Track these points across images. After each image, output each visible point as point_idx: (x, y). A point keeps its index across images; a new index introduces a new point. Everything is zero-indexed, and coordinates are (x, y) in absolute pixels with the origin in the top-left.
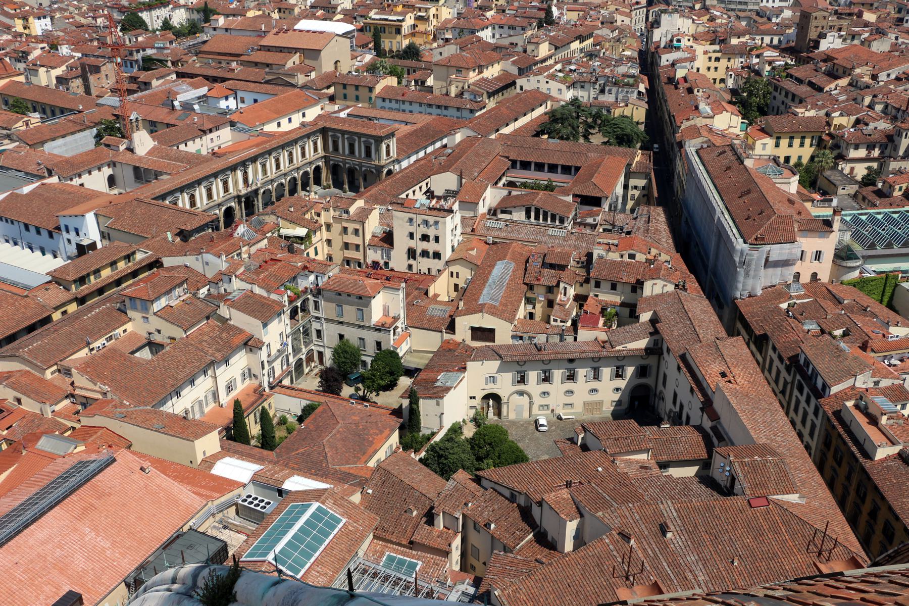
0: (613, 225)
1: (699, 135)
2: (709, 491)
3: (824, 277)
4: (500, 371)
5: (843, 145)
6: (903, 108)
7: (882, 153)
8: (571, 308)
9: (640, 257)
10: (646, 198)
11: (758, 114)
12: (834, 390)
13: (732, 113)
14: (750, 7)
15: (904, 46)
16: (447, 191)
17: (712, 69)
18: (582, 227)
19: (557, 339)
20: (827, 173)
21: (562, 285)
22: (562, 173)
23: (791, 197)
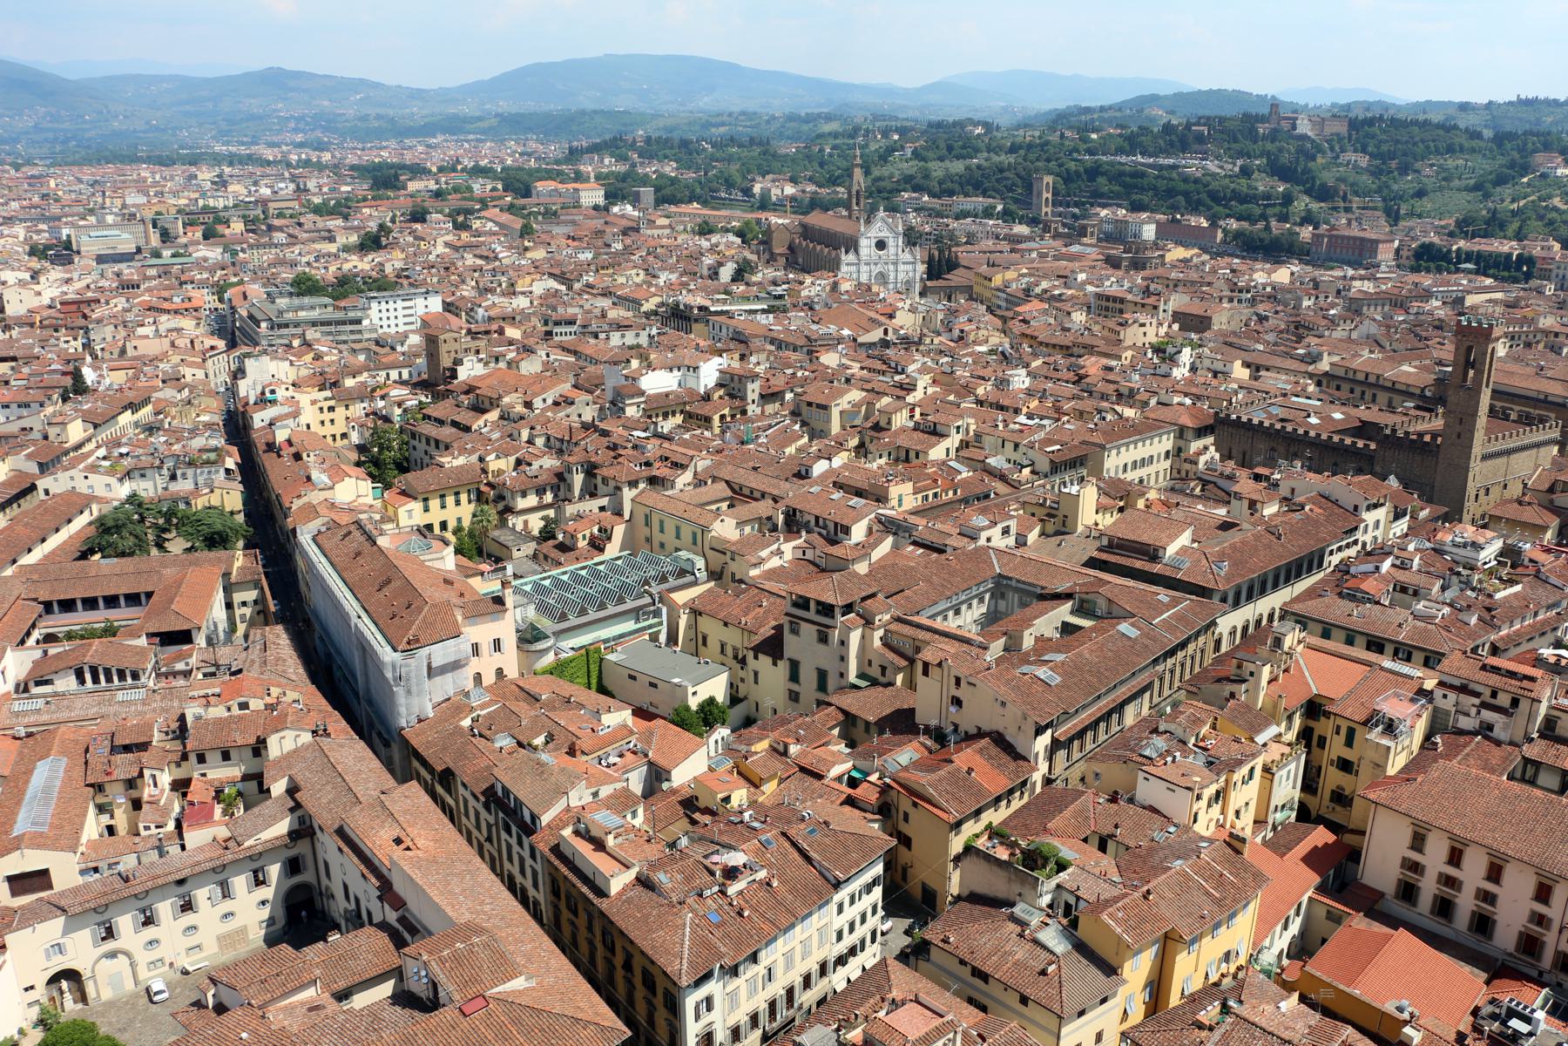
0: (217, 666)
1: (317, 515)
2: (408, 1011)
3: (512, 672)
5: (508, 495)
6: (567, 438)
7: (556, 496)
8: (170, 802)
9: (256, 704)
10: (262, 616)
12: (545, 819)
14: (367, 336)
15: (557, 364)
17: (327, 423)
18: (171, 678)
19: (154, 855)
20: (496, 534)
21: (147, 773)
22: (127, 606)
23: (449, 577)
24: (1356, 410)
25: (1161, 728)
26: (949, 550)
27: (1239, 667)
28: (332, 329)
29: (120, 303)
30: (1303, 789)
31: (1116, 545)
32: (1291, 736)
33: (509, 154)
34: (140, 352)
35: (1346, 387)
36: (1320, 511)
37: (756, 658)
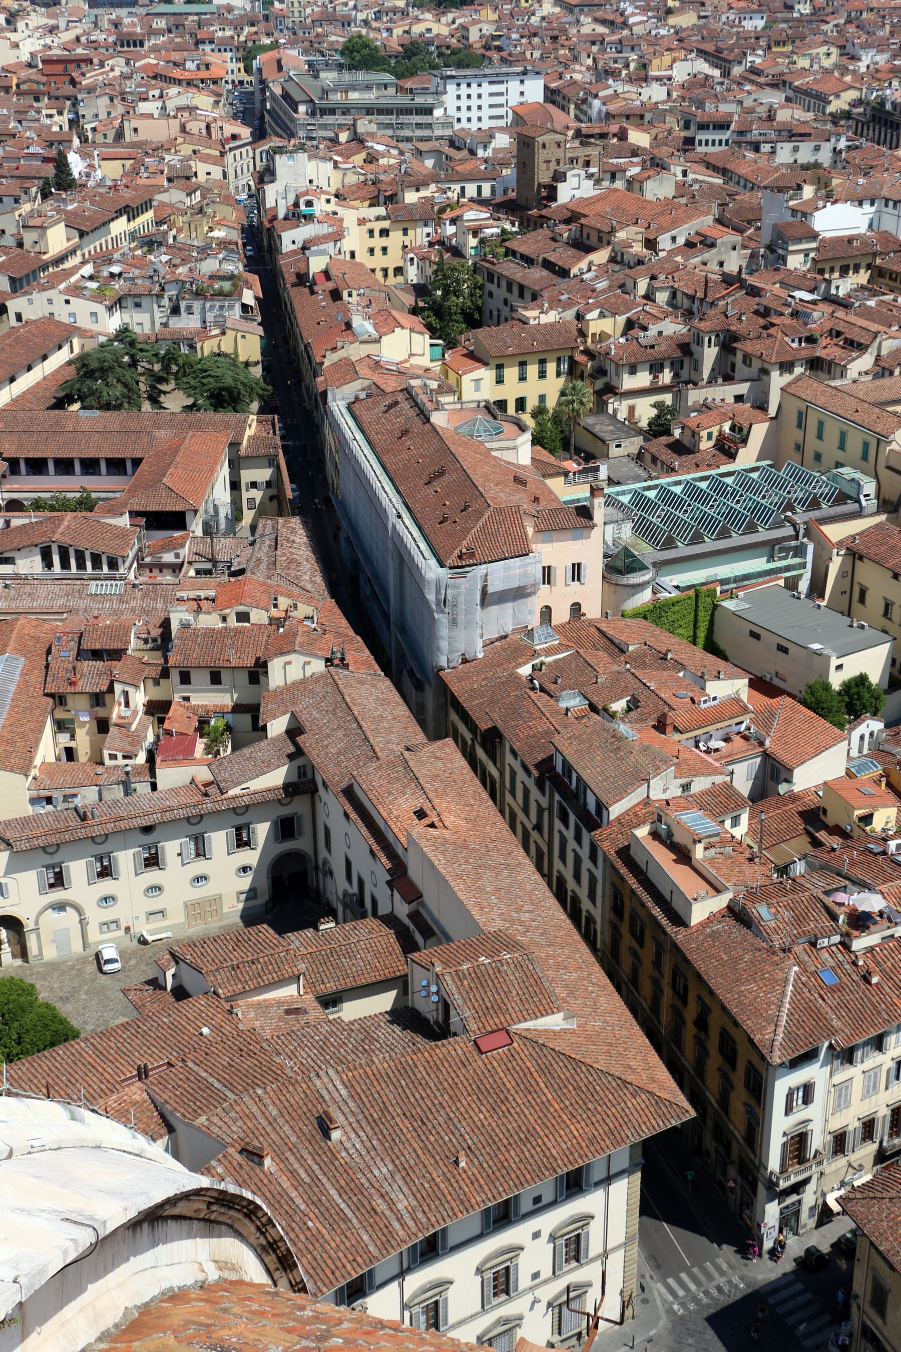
0: (214, 561)
1: (356, 376)
2: (408, 1035)
3: (592, 610)
4: (11, 869)
5: (611, 369)
6: (700, 295)
7: (676, 375)
8: (143, 727)
9: (258, 616)
10: (275, 502)
11: (464, 326)
12: (615, 811)
14: (438, 132)
15: (696, 187)
17: (378, 252)
18: (156, 571)
19: (119, 791)
20: (590, 421)
21: (118, 688)
22: (109, 474)
23: (521, 473)
28: (392, 119)
34: (142, 136)
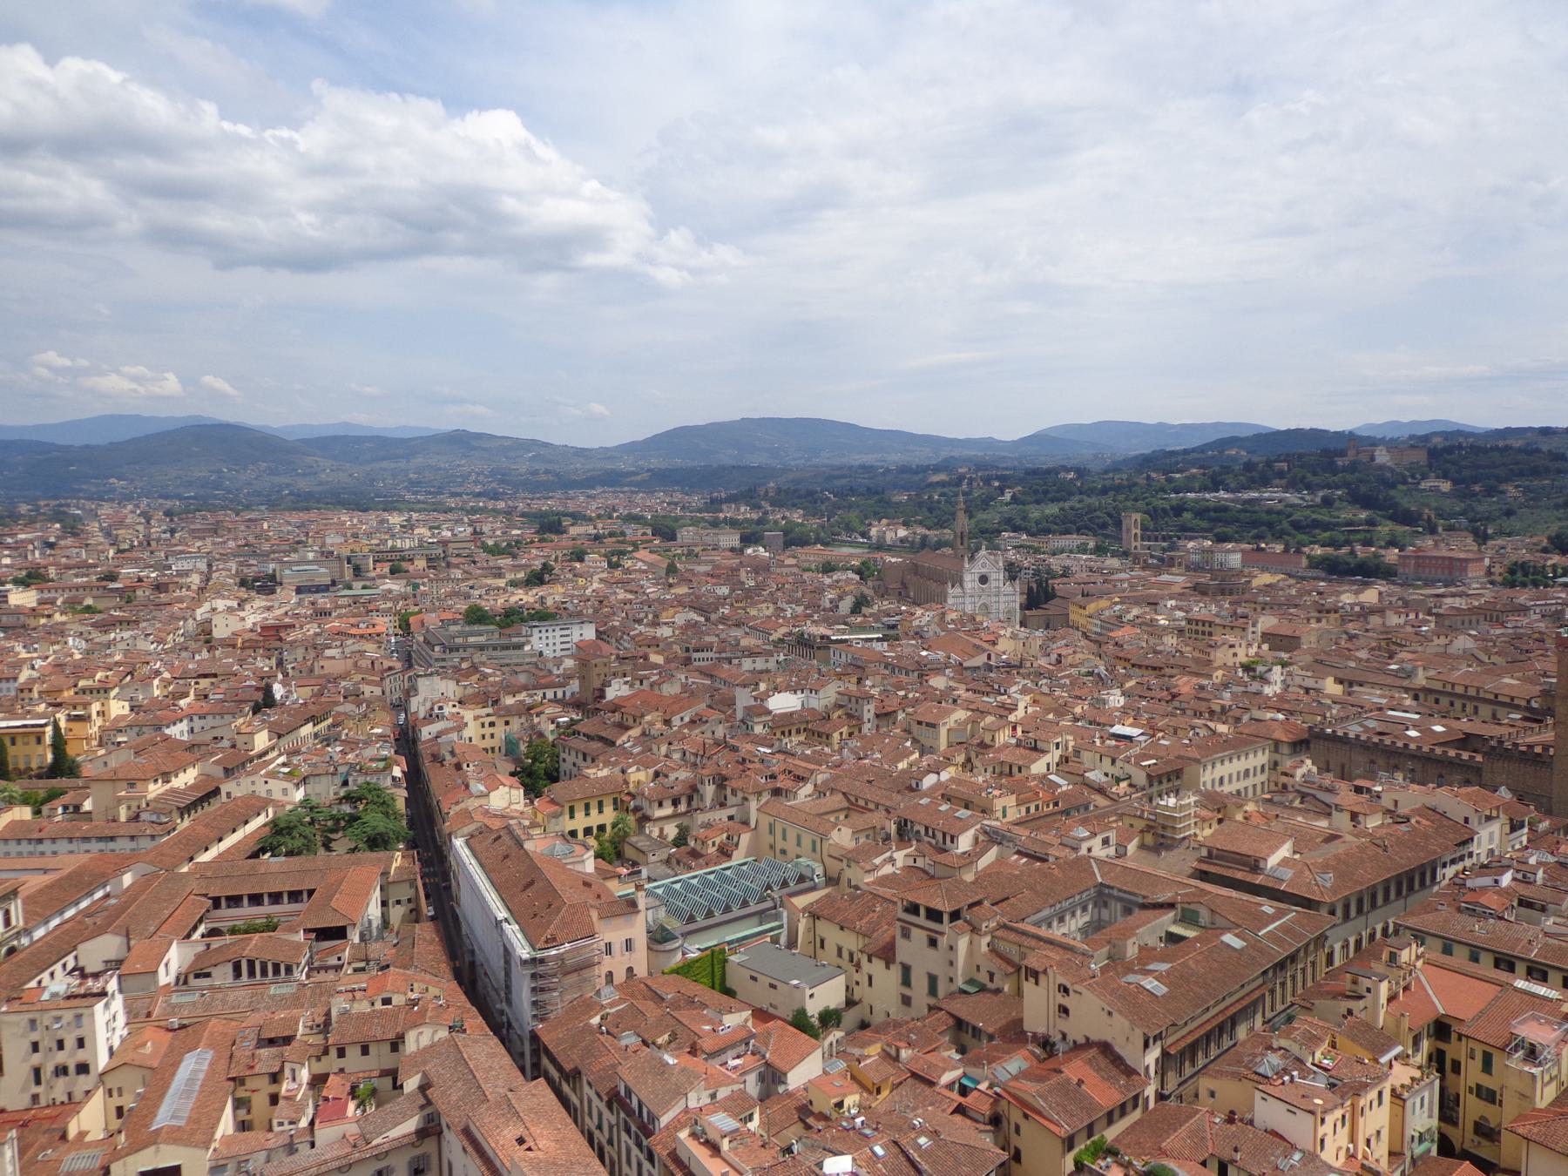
3: (641, 971)
6: (701, 753)
9: (398, 1000)
12: (664, 1120)
13: (511, 787)
16: (106, 962)
20: (633, 839)
23: (588, 879)
24: (1458, 722)
25: (1275, 1046)
26: (1051, 859)
27: (1355, 982)
29: (312, 629)
30: (1441, 1119)
31: (1213, 855)
32: (1420, 1058)
33: (654, 503)
34: (326, 671)
35: (1444, 701)
36: (1428, 823)
37: (870, 961)
